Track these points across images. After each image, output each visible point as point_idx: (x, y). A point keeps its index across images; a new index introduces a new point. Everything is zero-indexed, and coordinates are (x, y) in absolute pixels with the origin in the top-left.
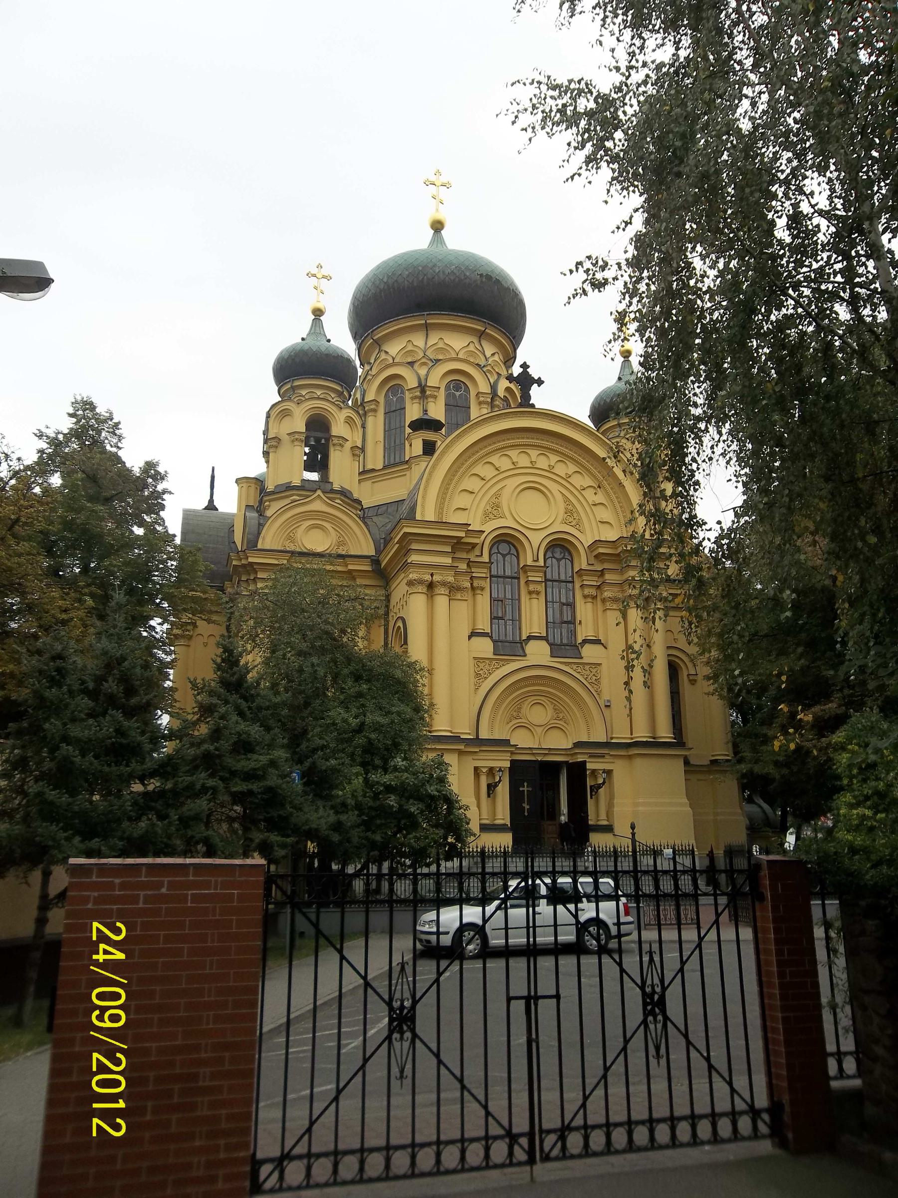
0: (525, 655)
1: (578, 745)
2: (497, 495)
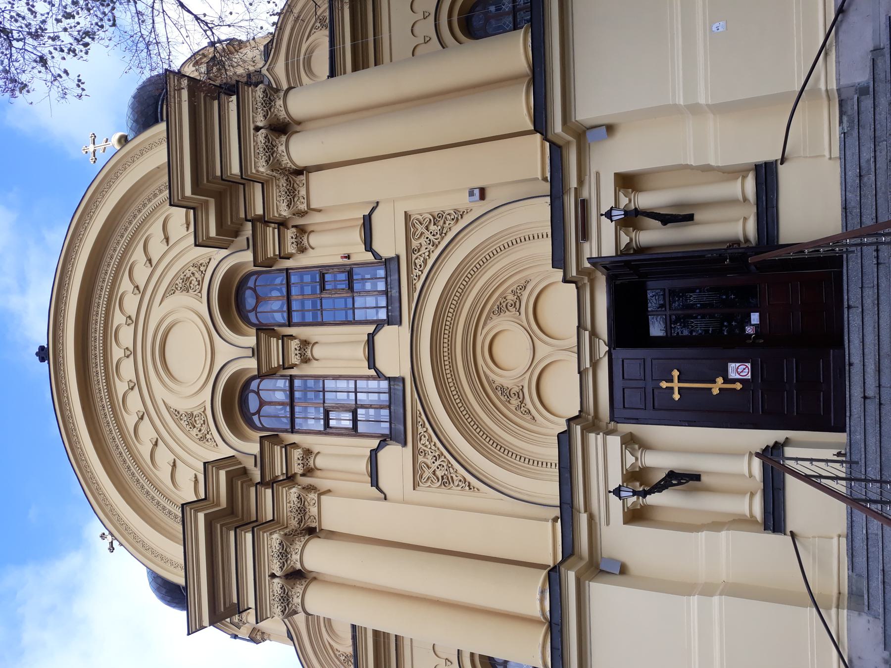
2: (176, 414)
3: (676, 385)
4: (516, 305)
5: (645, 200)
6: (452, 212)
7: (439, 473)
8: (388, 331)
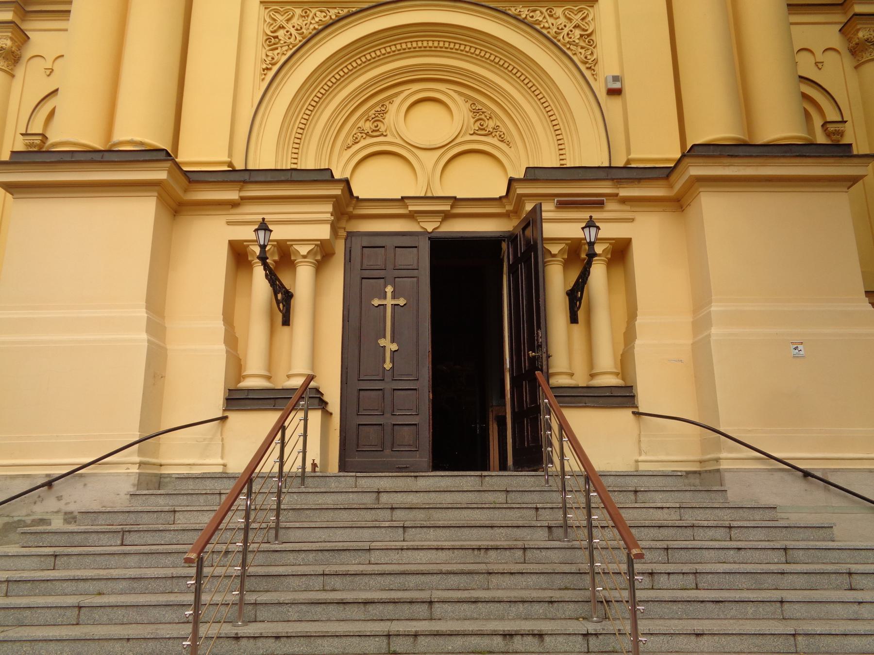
3: (389, 302)
4: (482, 131)
5: (598, 272)
6: (595, 57)
7: (281, 33)
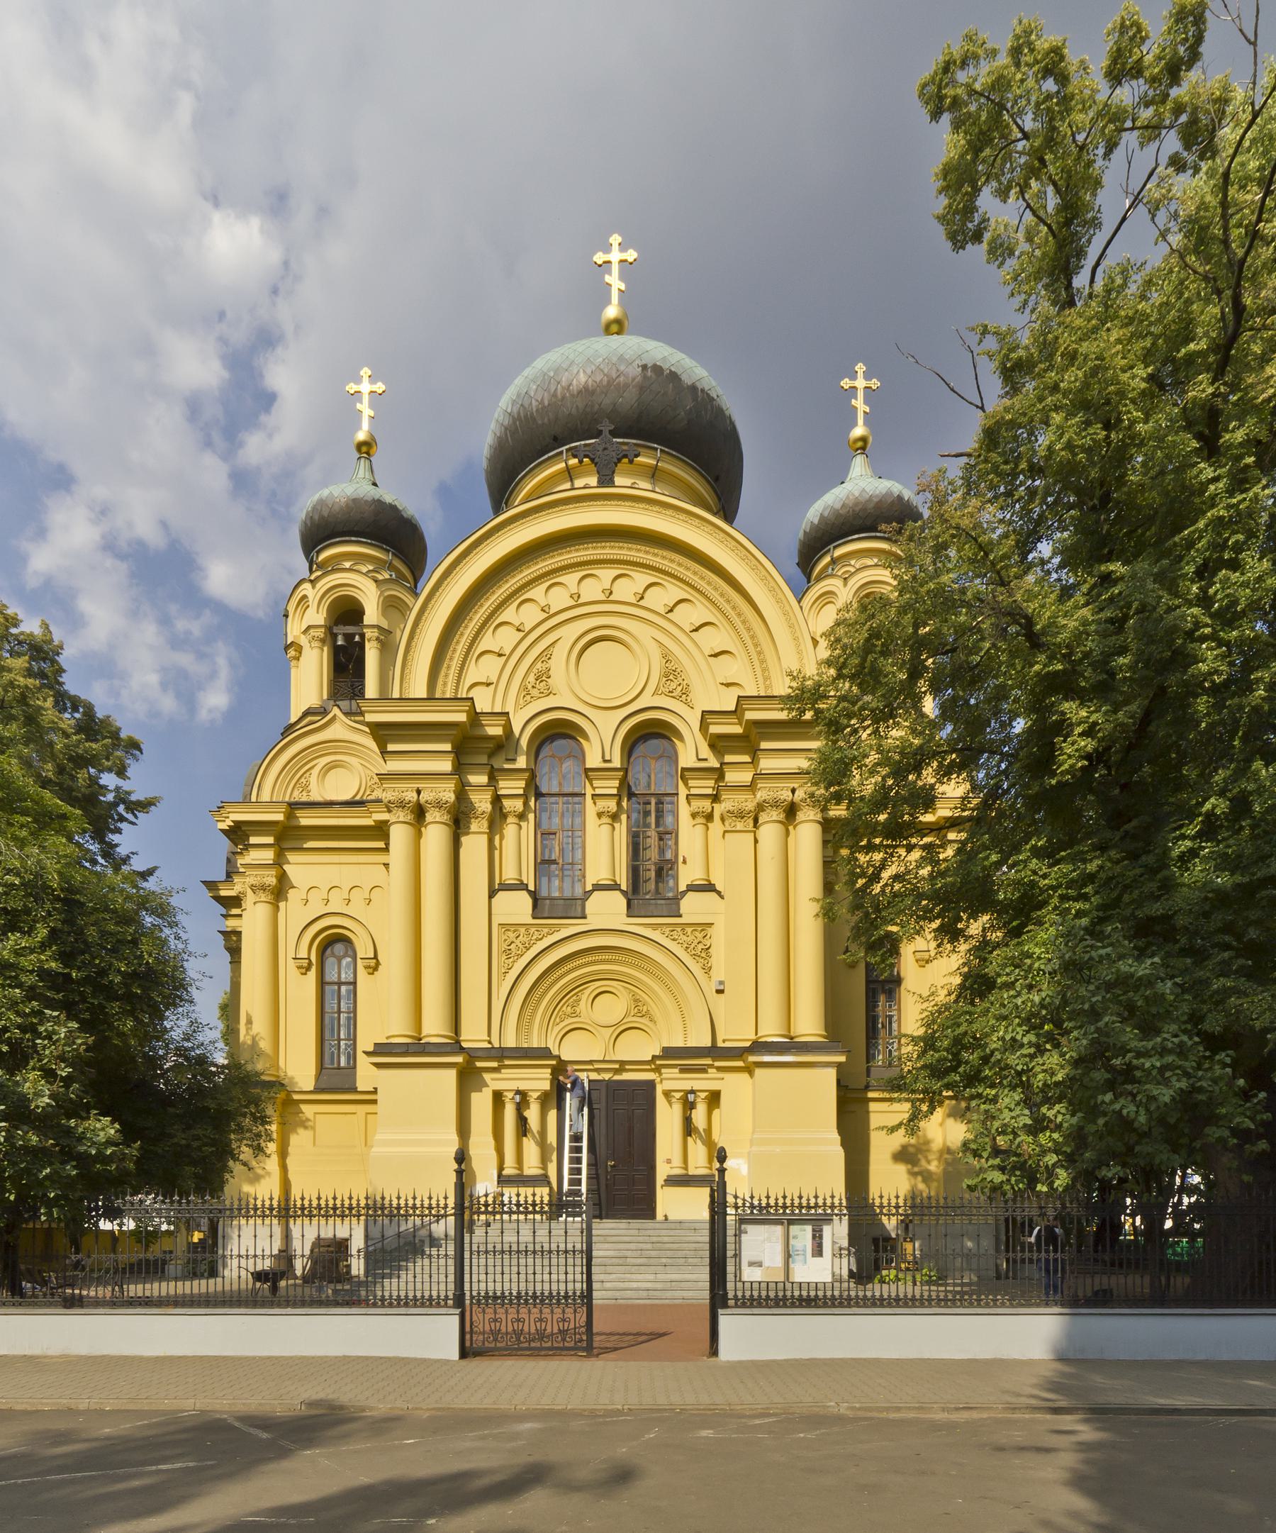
0: (584, 917)
1: (669, 1053)
8: (623, 902)
